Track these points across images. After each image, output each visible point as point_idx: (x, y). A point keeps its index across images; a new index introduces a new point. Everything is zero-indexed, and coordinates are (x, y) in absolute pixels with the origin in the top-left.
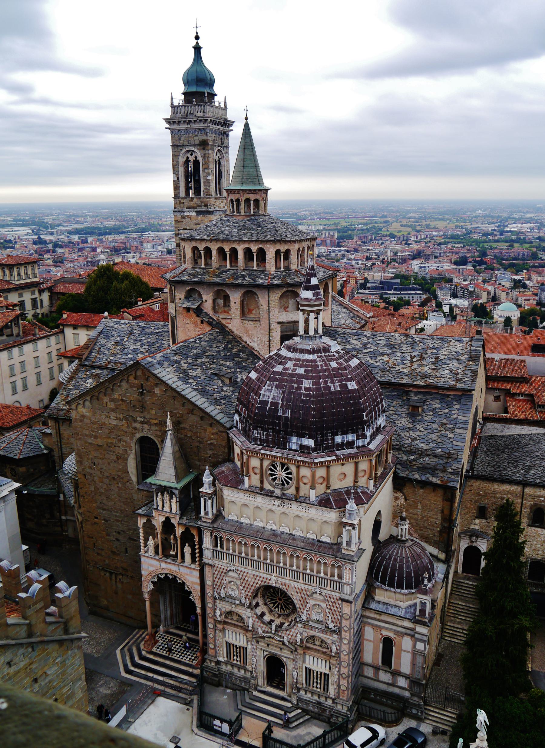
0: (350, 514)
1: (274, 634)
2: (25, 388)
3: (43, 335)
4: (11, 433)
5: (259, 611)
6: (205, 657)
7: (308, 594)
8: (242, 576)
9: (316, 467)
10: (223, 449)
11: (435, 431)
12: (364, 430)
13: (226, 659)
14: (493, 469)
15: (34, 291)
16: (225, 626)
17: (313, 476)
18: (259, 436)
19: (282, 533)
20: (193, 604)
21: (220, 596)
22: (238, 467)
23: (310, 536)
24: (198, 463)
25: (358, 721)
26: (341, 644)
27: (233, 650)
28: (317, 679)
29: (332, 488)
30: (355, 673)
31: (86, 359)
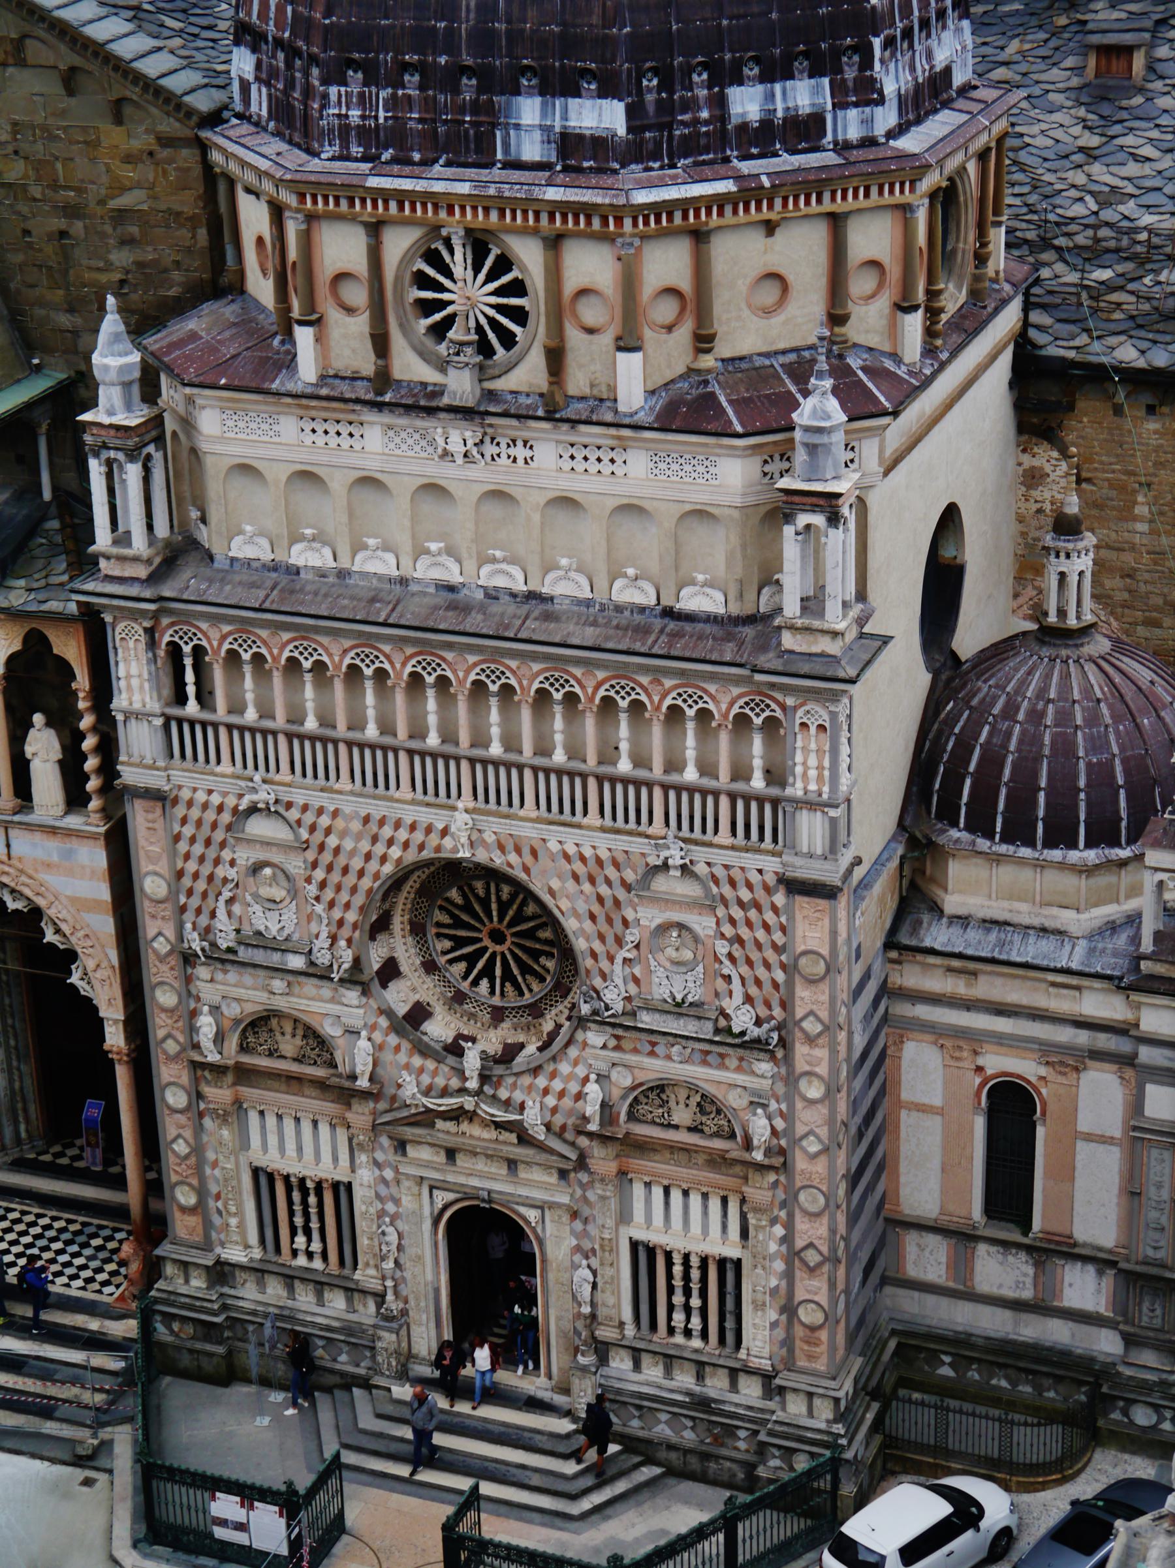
0: (812, 449)
1: (479, 1093)
5: (399, 996)
6: (158, 1252)
7: (630, 876)
8: (313, 828)
9: (644, 237)
10: (184, 233)
12: (867, 62)
13: (257, 1254)
16: (245, 1091)
17: (629, 282)
18: (355, 113)
19: (492, 595)
20: (88, 1008)
21: (213, 945)
22: (262, 309)
23: (625, 593)
24: (64, 320)
25: (882, 1478)
26: (791, 1106)
27: (290, 1203)
28: (687, 1293)
29: (724, 349)
30: (864, 1256)
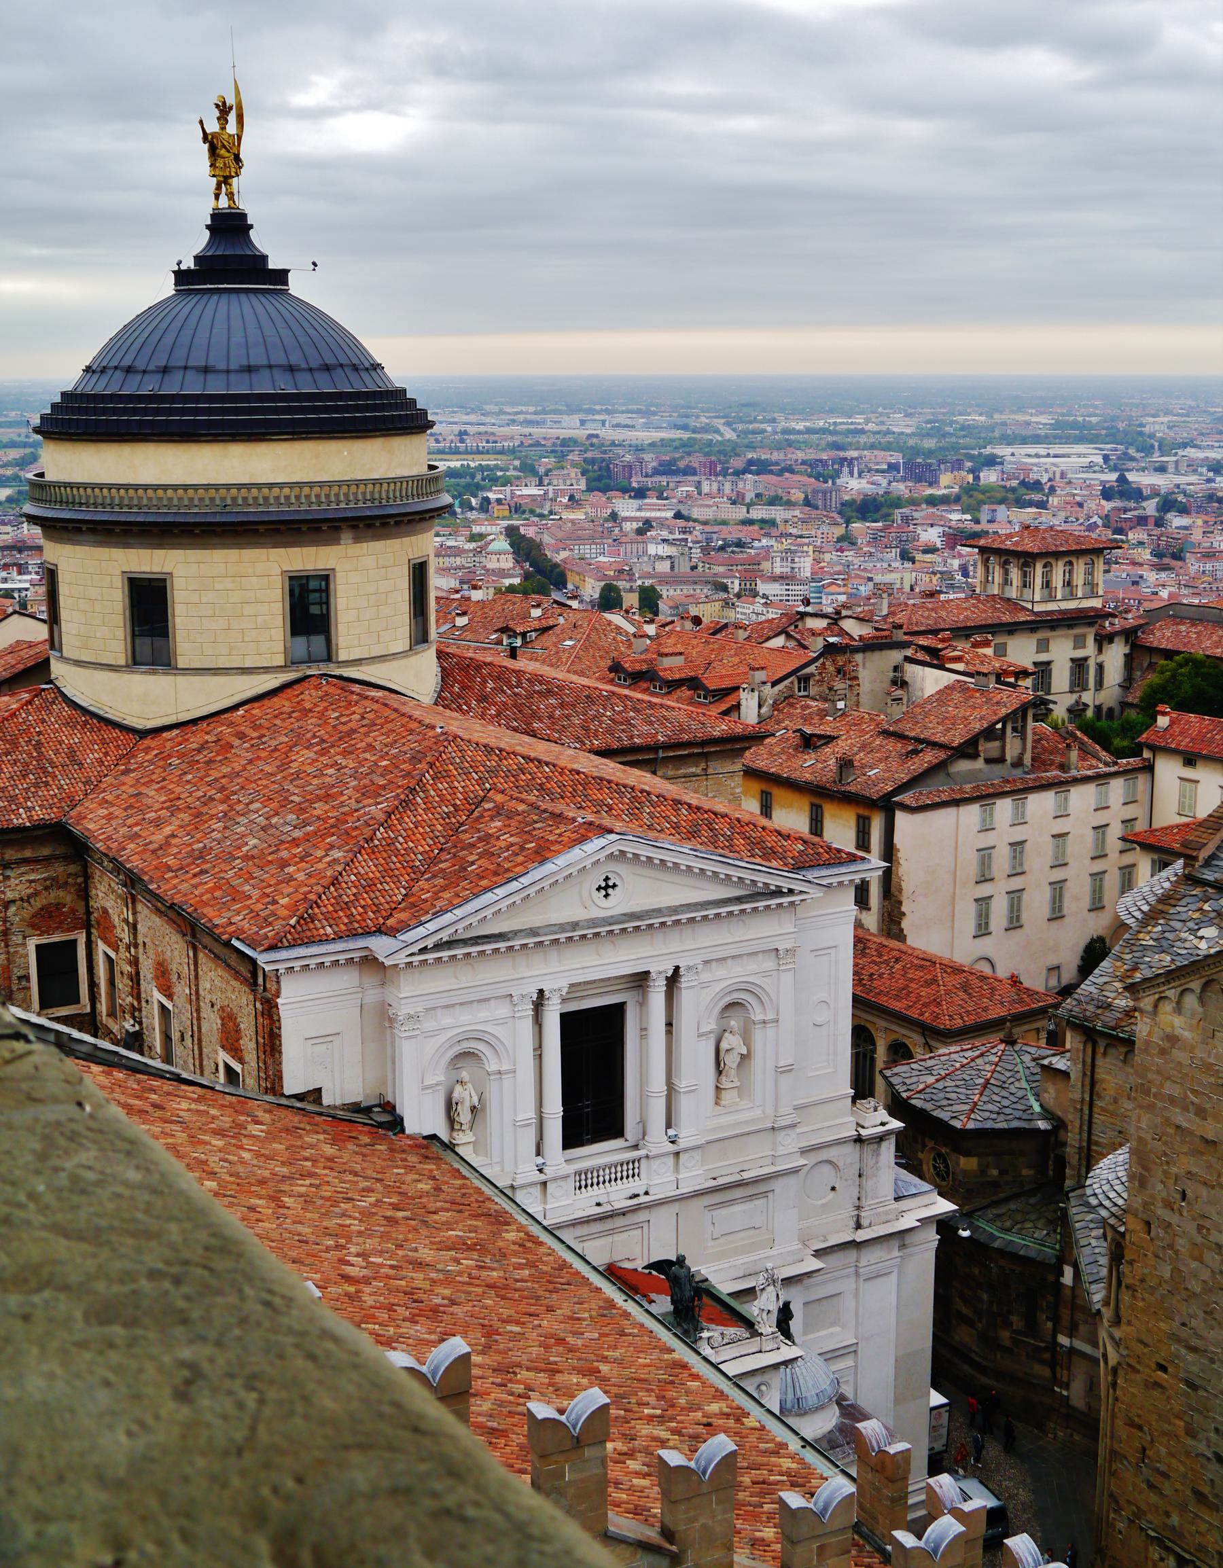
2: (1015, 923)
3: (1089, 773)
4: (953, 1049)
15: (1084, 636)
31: (1208, 863)
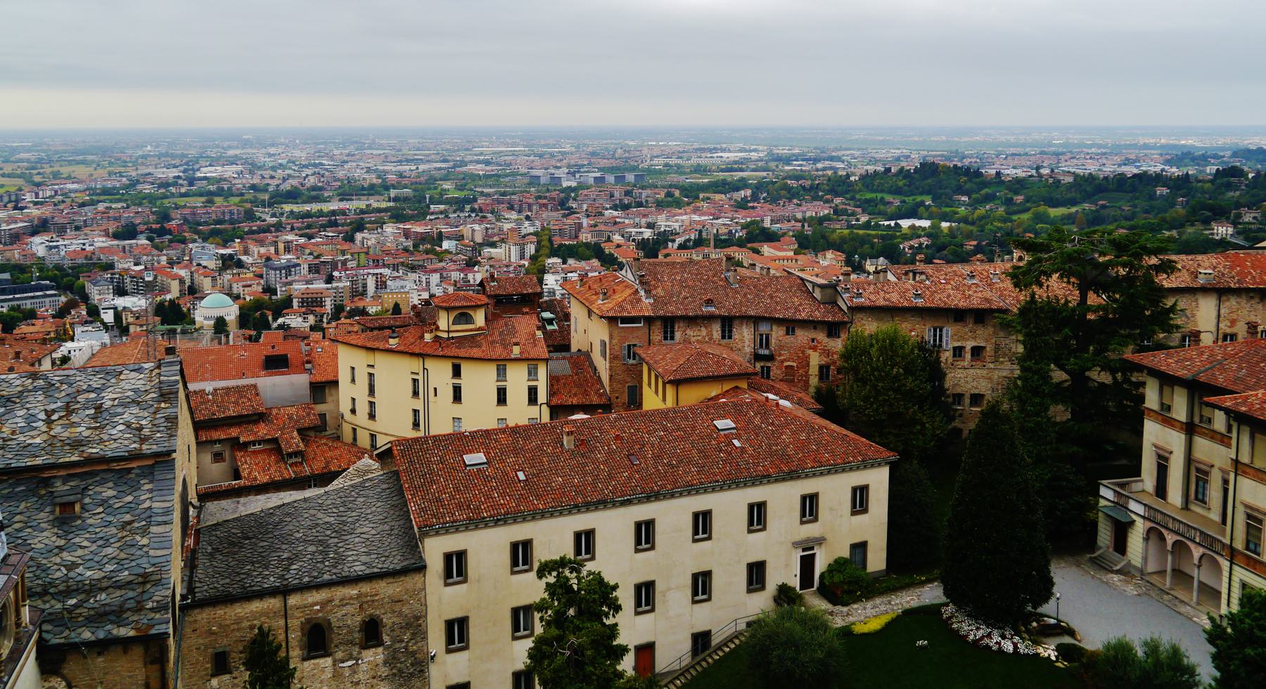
11: (112, 541)
14: (228, 581)
